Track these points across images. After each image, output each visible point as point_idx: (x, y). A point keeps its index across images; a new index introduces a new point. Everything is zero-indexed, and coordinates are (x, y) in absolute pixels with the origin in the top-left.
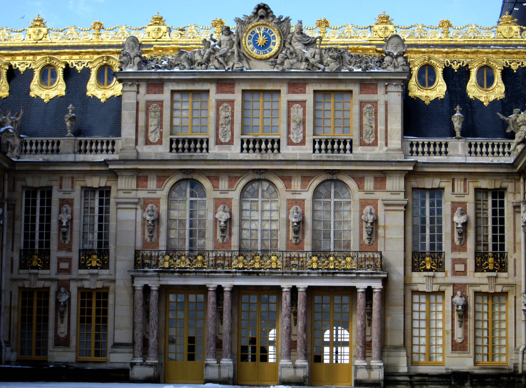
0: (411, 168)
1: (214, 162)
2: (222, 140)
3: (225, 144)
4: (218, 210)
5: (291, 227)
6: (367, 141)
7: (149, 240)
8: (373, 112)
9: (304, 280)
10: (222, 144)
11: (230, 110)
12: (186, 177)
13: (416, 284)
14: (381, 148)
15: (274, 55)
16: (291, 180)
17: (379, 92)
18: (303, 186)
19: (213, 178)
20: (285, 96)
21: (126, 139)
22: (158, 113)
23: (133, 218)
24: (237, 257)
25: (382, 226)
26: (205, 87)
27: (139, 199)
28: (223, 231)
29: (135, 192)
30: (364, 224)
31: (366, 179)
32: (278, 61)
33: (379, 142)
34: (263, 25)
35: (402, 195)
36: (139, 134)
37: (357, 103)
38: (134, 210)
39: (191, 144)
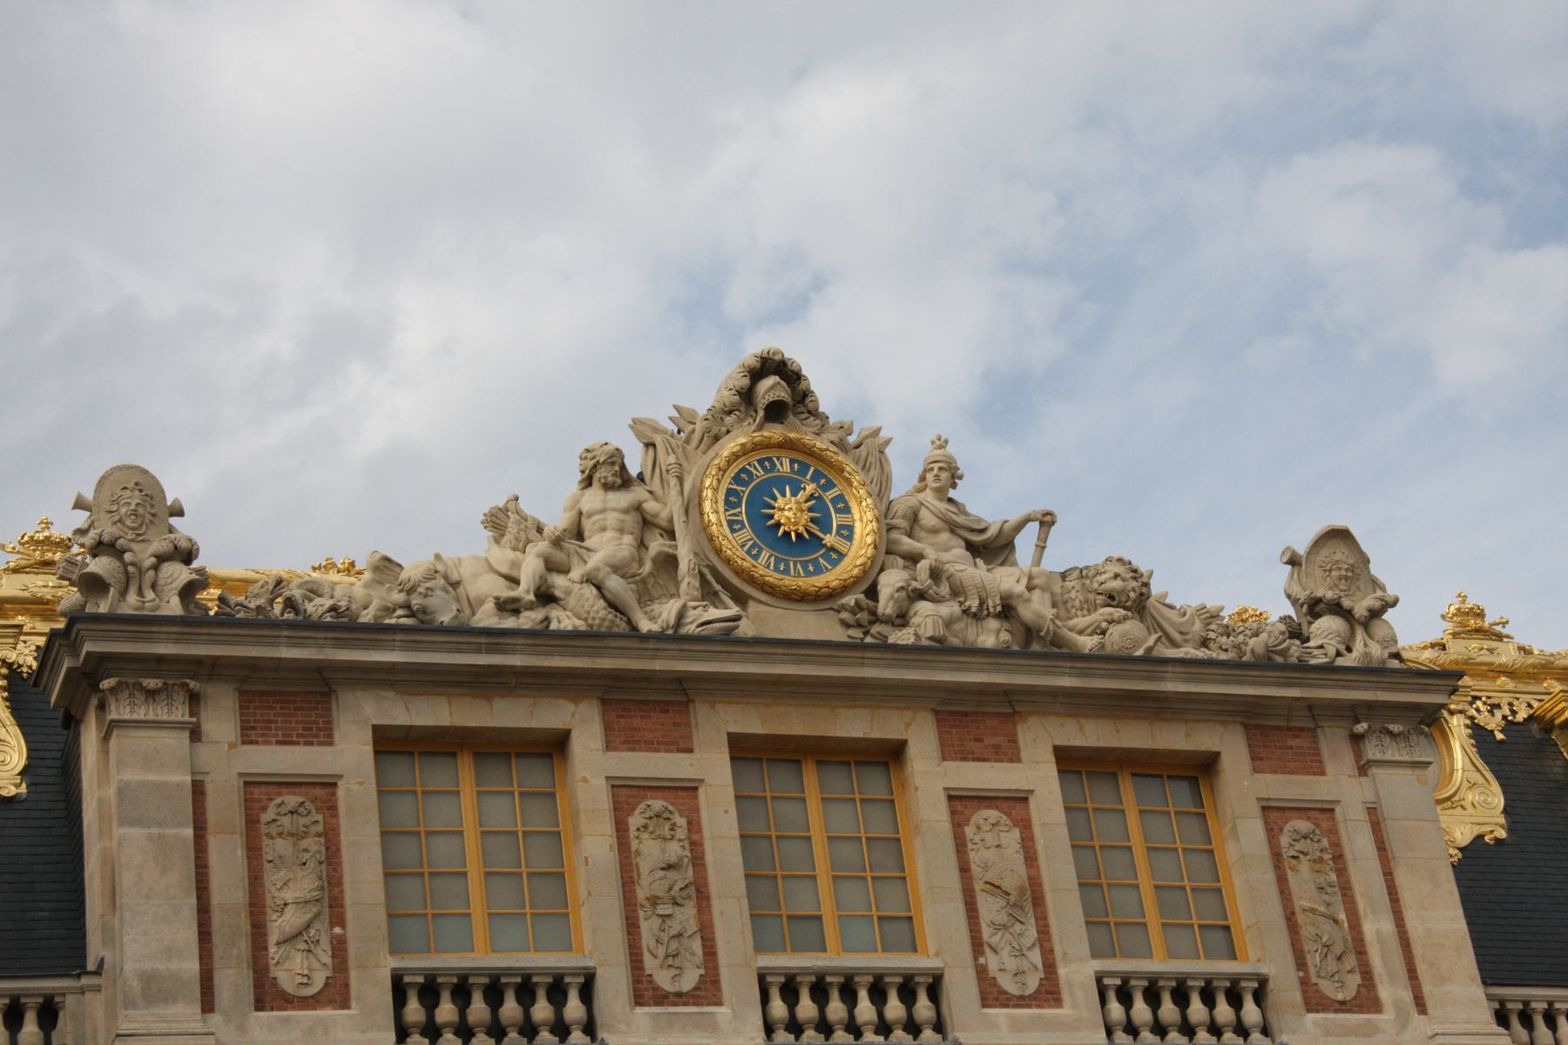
2: (664, 980)
3: (679, 994)
6: (1328, 988)
8: (1327, 857)
10: (661, 998)
11: (681, 833)
14: (1403, 1022)
15: (857, 580)
17: (1329, 769)
20: (930, 774)
21: (148, 979)
22: (304, 843)
26: (546, 715)
32: (885, 606)
33: (1385, 993)
34: (787, 445)
36: (217, 953)
37: (1254, 809)
39: (500, 1003)
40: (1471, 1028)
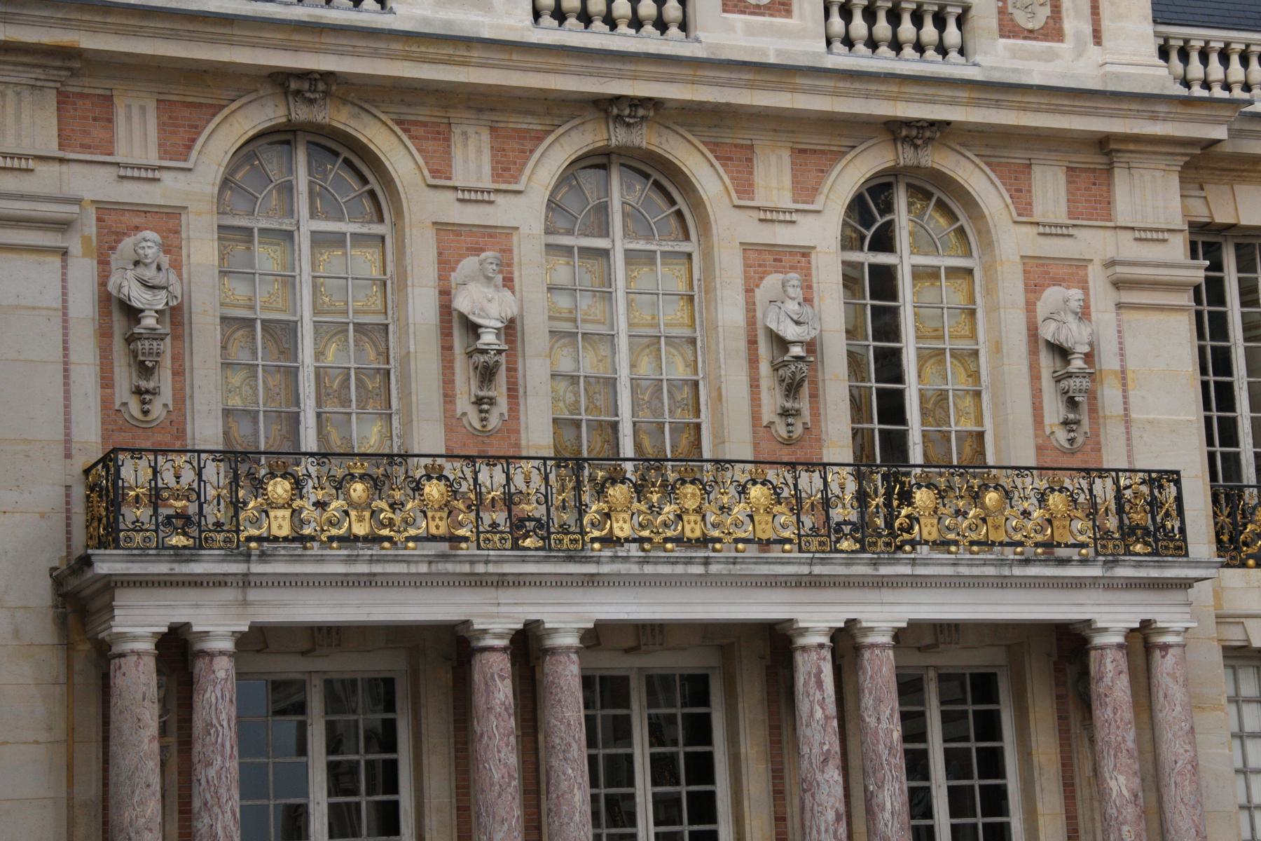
0: (1220, 133)
1: (447, 50)
4: (455, 277)
5: (764, 368)
6: (1021, 19)
7: (134, 408)
9: (887, 595)
12: (302, 114)
13: (1238, 619)
14: (1080, 52)
16: (750, 160)
18: (806, 190)
19: (421, 131)
23: (52, 298)
24: (600, 492)
25: (1115, 372)
27: (78, 201)
28: (487, 374)
29: (55, 168)
30: (1047, 362)
31: (1037, 172)
33: (1069, 25)
35: (1177, 248)
38: (56, 261)
40: (1136, 59)
